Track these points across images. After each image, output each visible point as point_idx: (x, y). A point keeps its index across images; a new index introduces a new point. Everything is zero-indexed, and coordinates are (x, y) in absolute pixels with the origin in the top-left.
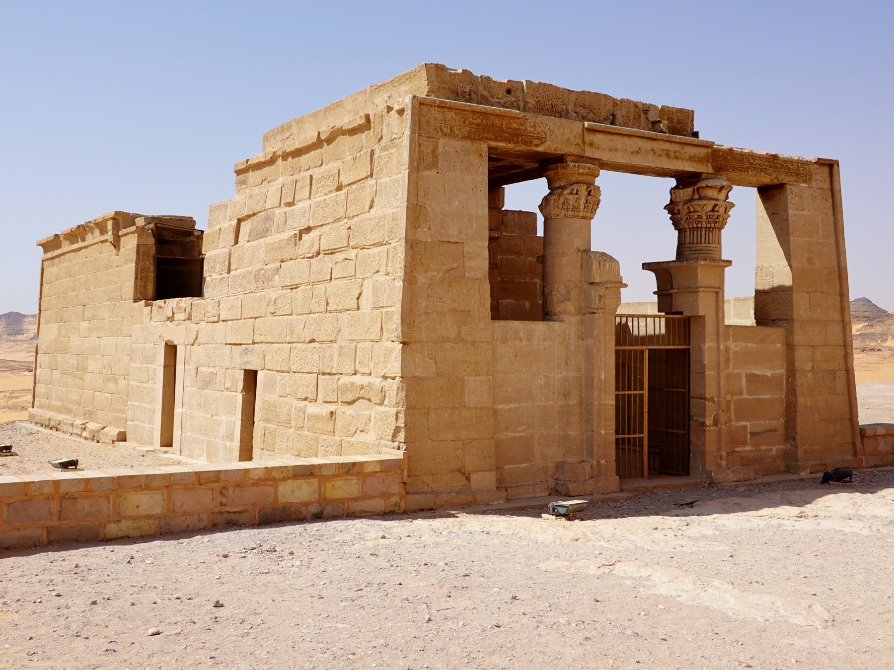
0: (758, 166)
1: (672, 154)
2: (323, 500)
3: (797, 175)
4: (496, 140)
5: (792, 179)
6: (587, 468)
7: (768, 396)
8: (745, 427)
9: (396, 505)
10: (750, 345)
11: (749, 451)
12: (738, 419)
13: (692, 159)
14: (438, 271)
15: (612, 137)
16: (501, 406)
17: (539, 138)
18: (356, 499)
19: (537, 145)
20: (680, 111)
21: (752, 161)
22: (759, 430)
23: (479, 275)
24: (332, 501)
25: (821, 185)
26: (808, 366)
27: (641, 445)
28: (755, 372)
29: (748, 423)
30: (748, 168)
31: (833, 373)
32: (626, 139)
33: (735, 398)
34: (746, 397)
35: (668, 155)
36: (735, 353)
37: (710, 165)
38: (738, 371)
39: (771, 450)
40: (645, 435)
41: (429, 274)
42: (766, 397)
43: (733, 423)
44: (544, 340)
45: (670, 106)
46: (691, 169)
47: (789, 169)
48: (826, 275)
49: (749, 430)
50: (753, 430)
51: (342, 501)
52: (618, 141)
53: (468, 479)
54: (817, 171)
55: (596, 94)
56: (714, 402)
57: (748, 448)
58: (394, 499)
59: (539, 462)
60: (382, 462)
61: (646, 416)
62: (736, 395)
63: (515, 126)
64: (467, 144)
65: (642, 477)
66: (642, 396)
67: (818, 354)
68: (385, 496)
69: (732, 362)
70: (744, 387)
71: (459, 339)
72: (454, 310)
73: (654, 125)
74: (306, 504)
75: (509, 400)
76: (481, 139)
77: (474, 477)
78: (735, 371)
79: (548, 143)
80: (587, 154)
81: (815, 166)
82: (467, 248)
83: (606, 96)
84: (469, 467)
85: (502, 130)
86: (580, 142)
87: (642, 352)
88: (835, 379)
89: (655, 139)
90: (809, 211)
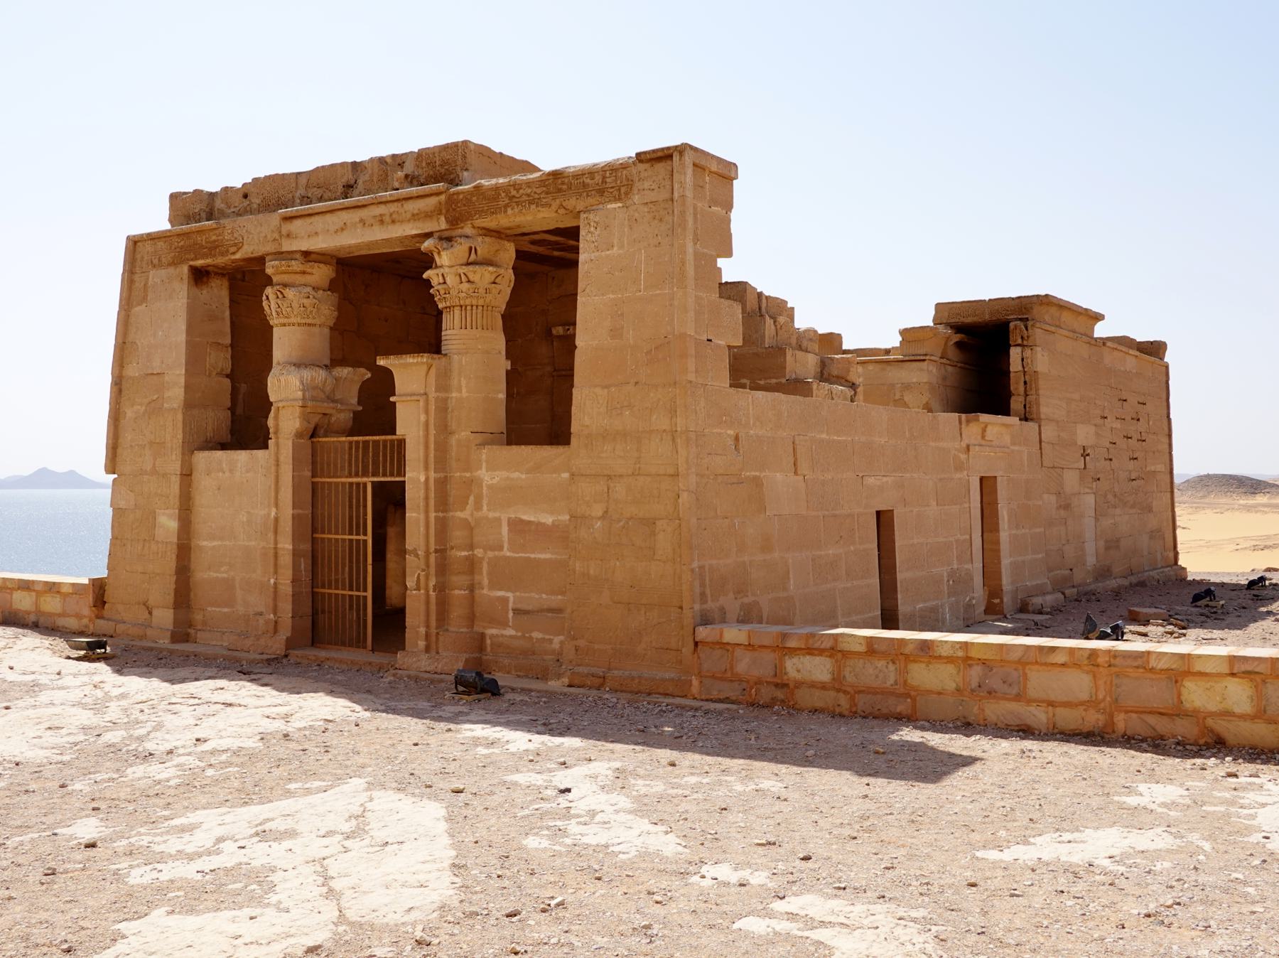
0: (525, 198)
1: (387, 219)
2: (39, 612)
3: (601, 192)
4: (196, 259)
5: (591, 201)
6: (261, 621)
7: (548, 556)
8: (506, 600)
9: (86, 626)
10: (516, 475)
11: (511, 637)
12: (493, 586)
13: (415, 217)
14: (141, 405)
15: (309, 220)
16: (205, 543)
17: (235, 245)
18: (59, 615)
19: (234, 253)
20: (446, 147)
21: (514, 193)
22: (530, 608)
23: (175, 406)
24: (43, 614)
25: (652, 196)
26: (598, 510)
27: (365, 605)
28: (525, 517)
29: (510, 595)
30: (506, 206)
31: (650, 523)
32: (328, 216)
33: (490, 554)
34: (508, 554)
35: (382, 222)
36: (490, 487)
37: (443, 218)
38: (497, 515)
39: (551, 641)
40: (369, 594)
41: (137, 407)
42: (542, 556)
43: (485, 591)
44: (247, 472)
45: (431, 145)
46: (414, 232)
47: (585, 185)
48: (649, 352)
49: (511, 605)
50: (519, 606)
51: (51, 615)
52: (318, 222)
53: (150, 613)
54: (643, 175)
55: (332, 165)
56: (417, 556)
57: (510, 632)
58: (85, 621)
59: (241, 610)
60: (73, 585)
61: (370, 568)
62: (492, 549)
63: (214, 238)
64: (171, 270)
65: (365, 647)
66: (365, 541)
67: (620, 490)
68: (78, 616)
69: (485, 502)
70: (506, 539)
71: (154, 472)
72: (151, 443)
73: (411, 180)
74: (29, 613)
75: (212, 537)
76: (182, 262)
77: (155, 612)
78: (491, 515)
79: (245, 247)
80: (284, 249)
81: (641, 167)
82: (167, 378)
83: (343, 164)
84: (151, 603)
85: (202, 247)
86: (276, 235)
87: (365, 485)
88: (653, 534)
89: (364, 206)
90: (621, 247)
